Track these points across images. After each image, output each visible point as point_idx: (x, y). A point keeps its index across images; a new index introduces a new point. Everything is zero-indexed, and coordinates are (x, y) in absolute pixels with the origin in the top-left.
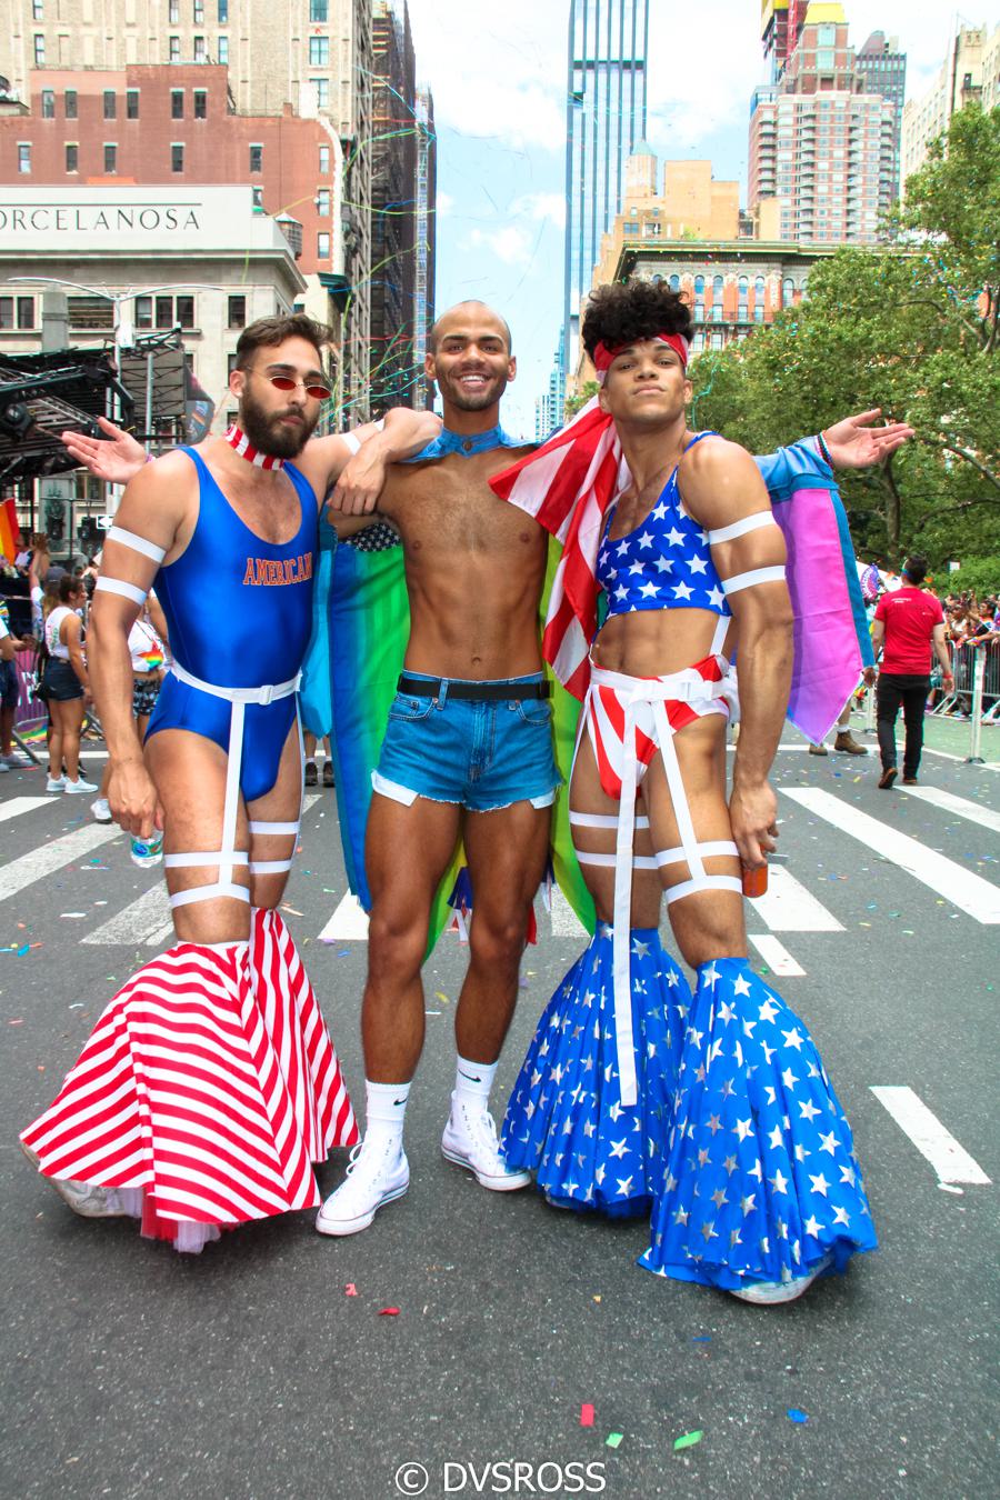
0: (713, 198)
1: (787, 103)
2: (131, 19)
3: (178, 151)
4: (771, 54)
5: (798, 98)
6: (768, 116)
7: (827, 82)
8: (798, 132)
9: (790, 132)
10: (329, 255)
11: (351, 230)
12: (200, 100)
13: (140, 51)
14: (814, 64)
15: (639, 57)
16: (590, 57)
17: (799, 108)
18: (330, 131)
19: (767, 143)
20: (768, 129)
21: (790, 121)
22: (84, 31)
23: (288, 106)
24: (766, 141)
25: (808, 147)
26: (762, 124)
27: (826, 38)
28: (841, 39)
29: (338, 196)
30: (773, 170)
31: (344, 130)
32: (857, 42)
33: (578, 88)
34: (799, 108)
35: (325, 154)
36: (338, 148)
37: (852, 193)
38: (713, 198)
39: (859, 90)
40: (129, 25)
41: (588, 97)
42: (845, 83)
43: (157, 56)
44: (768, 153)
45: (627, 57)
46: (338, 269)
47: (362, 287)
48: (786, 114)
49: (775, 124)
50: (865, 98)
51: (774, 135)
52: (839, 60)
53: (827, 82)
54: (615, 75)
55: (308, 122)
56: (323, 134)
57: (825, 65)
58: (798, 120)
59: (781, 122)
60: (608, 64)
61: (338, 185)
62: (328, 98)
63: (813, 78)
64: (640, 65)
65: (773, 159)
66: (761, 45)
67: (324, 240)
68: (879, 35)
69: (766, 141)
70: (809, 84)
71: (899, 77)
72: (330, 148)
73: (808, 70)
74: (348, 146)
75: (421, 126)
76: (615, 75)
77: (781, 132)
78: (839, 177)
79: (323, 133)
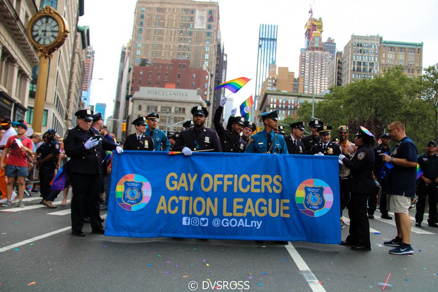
0: (289, 76)
1: (308, 53)
2: (171, 49)
3: (179, 74)
4: (307, 38)
5: (310, 52)
6: (304, 55)
7: (317, 49)
8: (310, 59)
9: (308, 59)
10: (206, 95)
11: (211, 90)
12: (184, 65)
13: (173, 55)
14: (314, 44)
15: (275, 38)
16: (264, 37)
17: (310, 54)
18: (208, 72)
19: (303, 61)
20: (304, 58)
21: (308, 56)
22: (163, 51)
23: (201, 68)
24: (303, 60)
25: (313, 62)
26: (302, 56)
27: (317, 39)
28: (320, 39)
29: (209, 85)
30: (305, 67)
31: (211, 72)
32: (324, 40)
33: (260, 44)
34: (310, 54)
35: (207, 77)
36: (210, 75)
37: (323, 68)
38: (289, 76)
39: (324, 51)
40: (171, 50)
41: (263, 46)
42: (321, 49)
43: (175, 57)
44: (304, 63)
45: (272, 38)
46: (208, 100)
47: (212, 102)
48: (307, 55)
49: (305, 57)
50: (326, 53)
51: (305, 59)
52: (320, 44)
53: (317, 49)
54: (269, 42)
55: (205, 71)
56: (208, 75)
57: (317, 45)
58: (310, 57)
59: (306, 56)
60: (268, 39)
61: (209, 83)
62: (208, 65)
63: (314, 48)
64: (276, 40)
65: (305, 64)
66: (304, 36)
67: (206, 93)
68: (330, 38)
69: (303, 60)
70: (313, 49)
71: (334, 47)
72: (208, 76)
73: (313, 46)
74: (212, 76)
75: (225, 61)
76: (269, 42)
77: (306, 59)
78: (319, 70)
79: (207, 73)
